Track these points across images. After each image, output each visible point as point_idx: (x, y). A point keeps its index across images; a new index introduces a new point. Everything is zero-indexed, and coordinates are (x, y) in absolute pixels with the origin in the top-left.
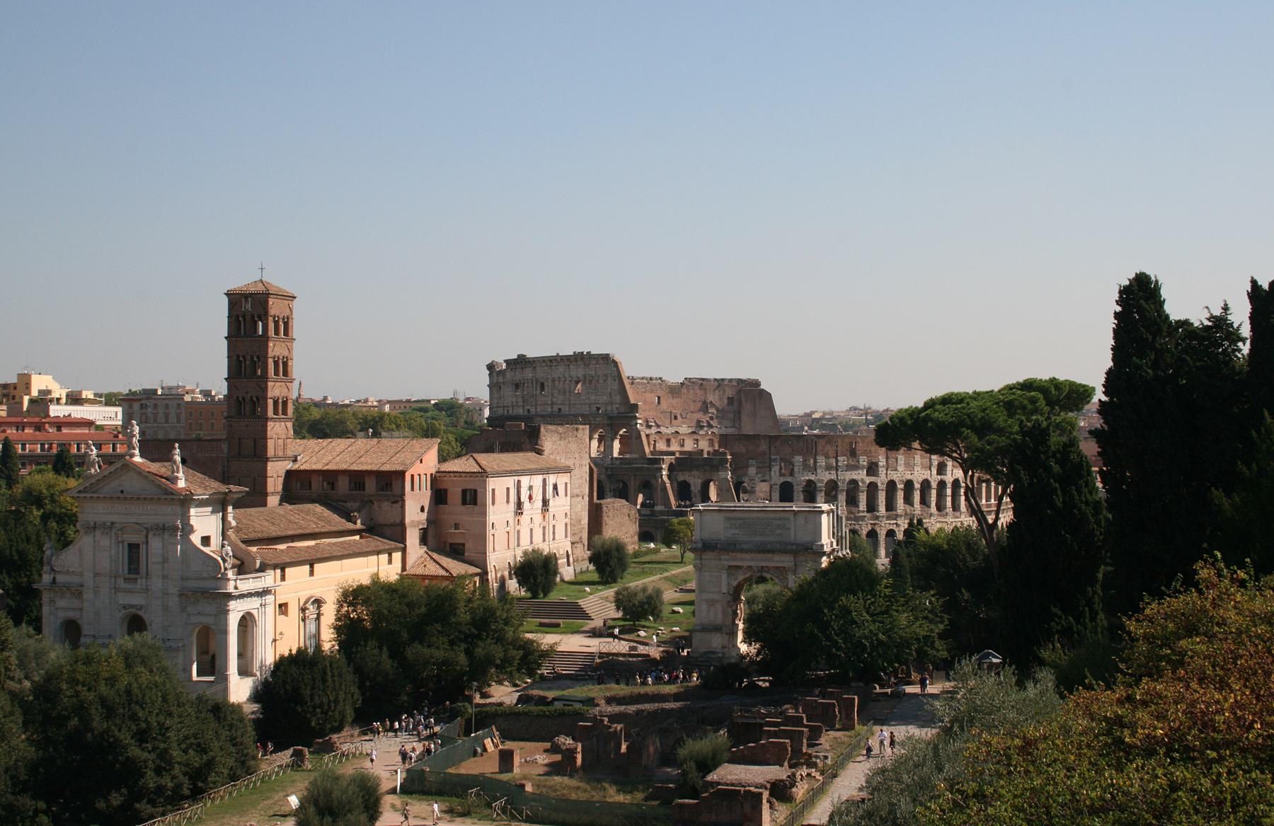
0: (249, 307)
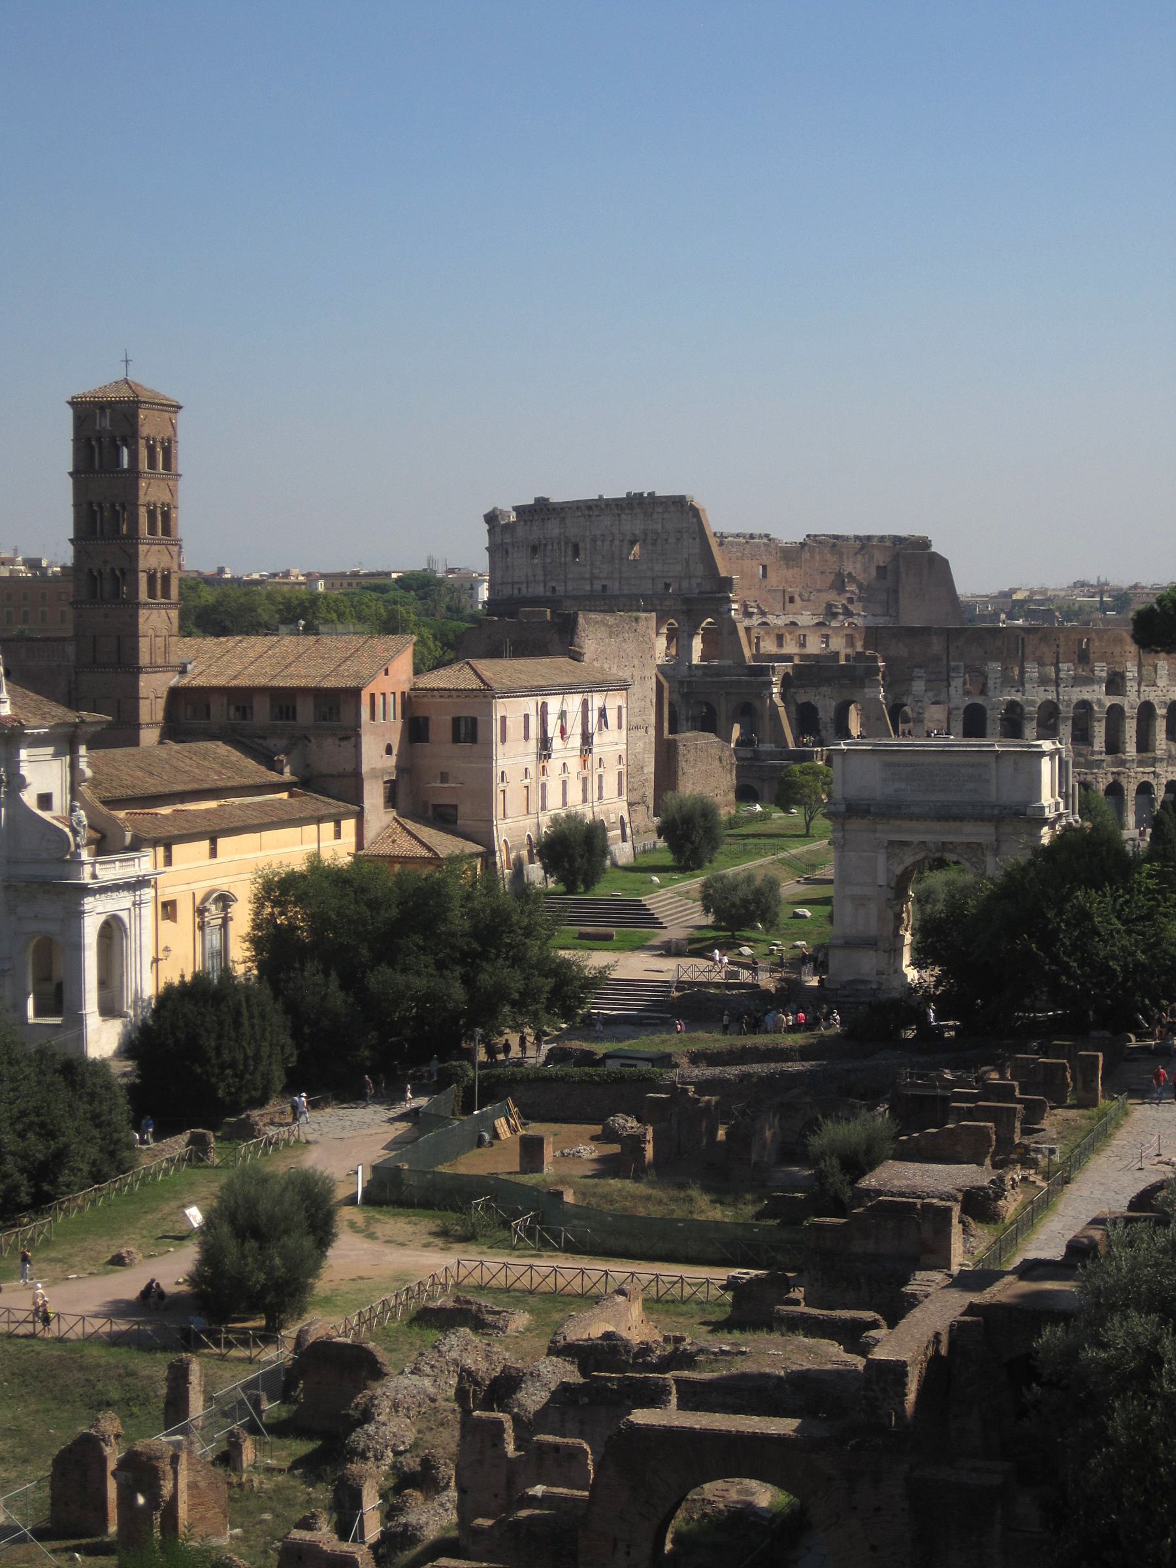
0: (107, 423)
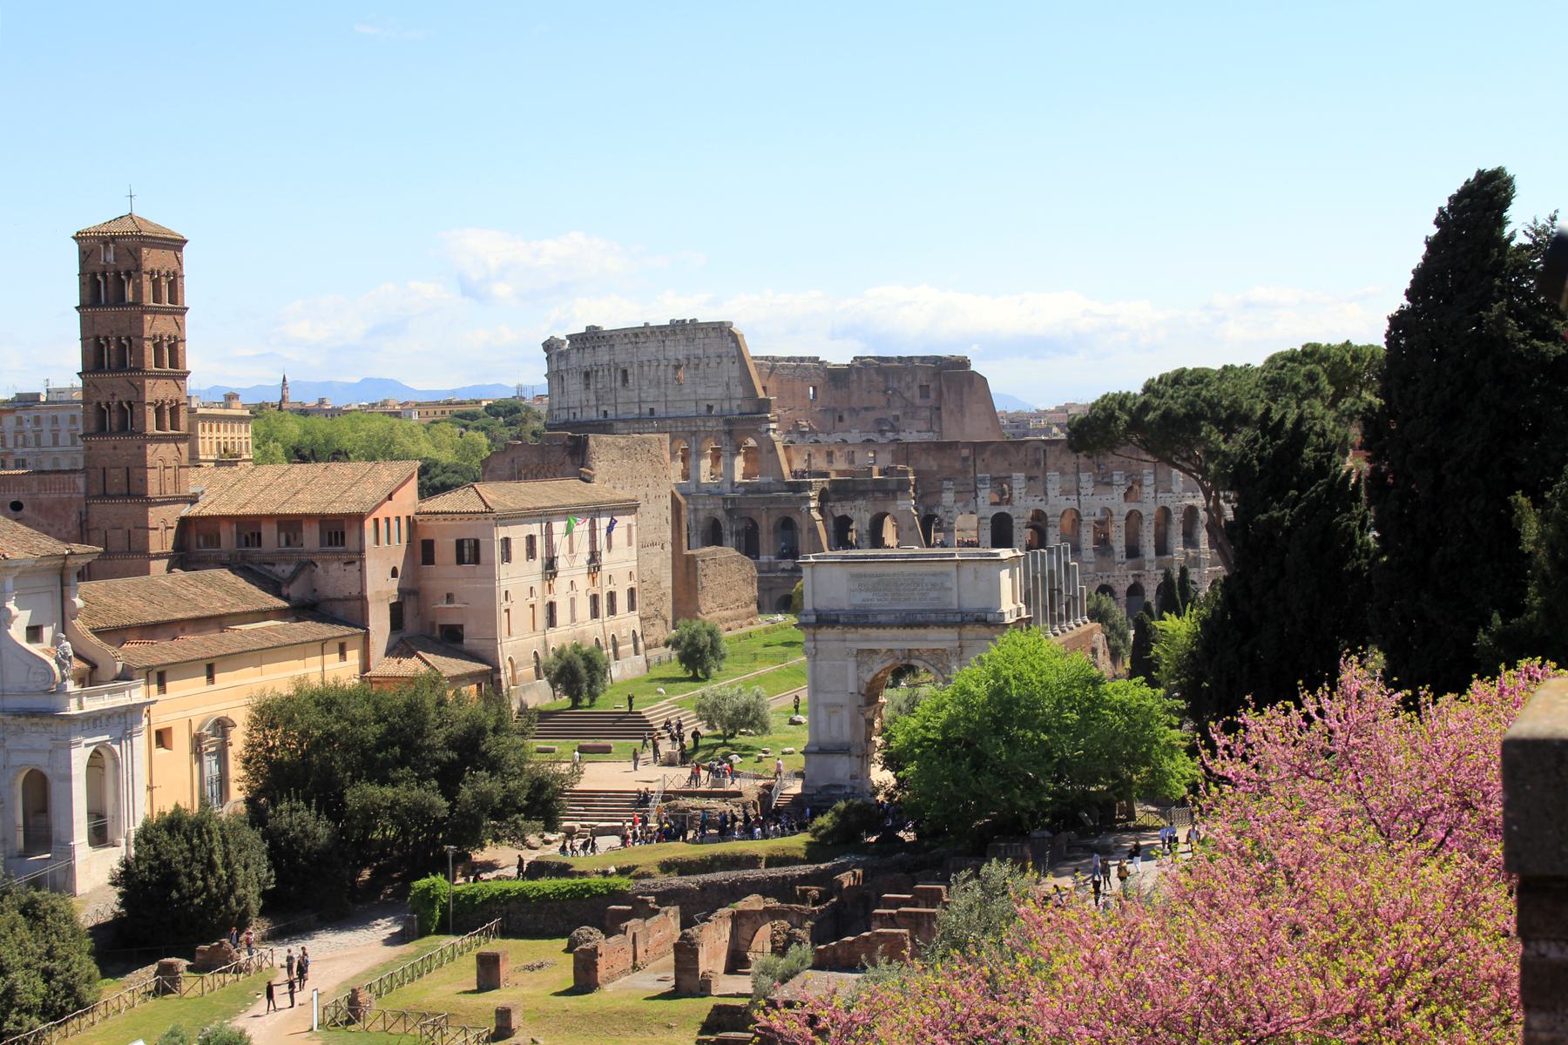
0: (110, 257)
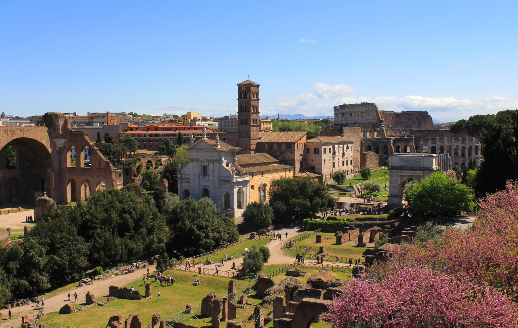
0: (244, 89)
